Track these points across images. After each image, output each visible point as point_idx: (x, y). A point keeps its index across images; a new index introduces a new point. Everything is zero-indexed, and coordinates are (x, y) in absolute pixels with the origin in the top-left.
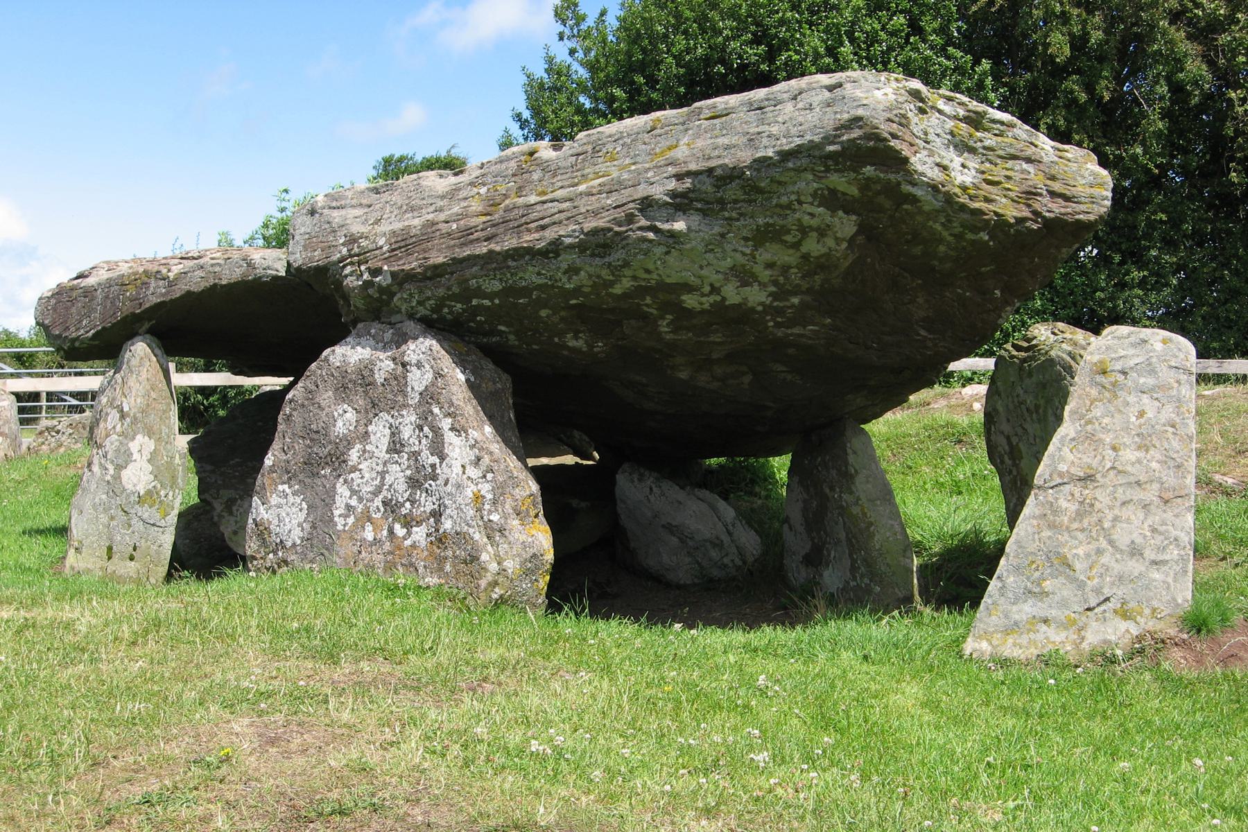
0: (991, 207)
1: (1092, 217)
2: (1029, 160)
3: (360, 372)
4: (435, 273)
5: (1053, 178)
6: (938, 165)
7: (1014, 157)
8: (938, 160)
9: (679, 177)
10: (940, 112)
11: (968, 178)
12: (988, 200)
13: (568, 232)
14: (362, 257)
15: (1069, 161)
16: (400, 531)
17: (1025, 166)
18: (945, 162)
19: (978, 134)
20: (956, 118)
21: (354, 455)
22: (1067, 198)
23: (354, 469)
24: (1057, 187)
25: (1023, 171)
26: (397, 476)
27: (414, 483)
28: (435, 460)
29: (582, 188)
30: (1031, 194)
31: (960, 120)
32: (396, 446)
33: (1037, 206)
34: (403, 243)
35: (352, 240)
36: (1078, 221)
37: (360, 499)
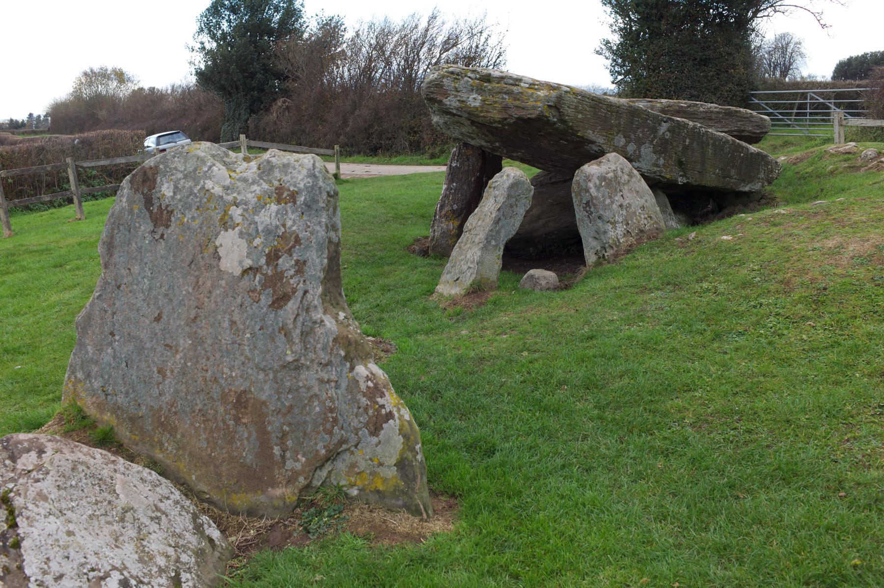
0: (489, 115)
1: (533, 116)
2: (506, 93)
5: (518, 100)
6: (459, 101)
7: (500, 93)
8: (459, 98)
10: (470, 77)
11: (477, 104)
12: (487, 112)
15: (536, 89)
17: (505, 96)
18: (464, 99)
19: (485, 84)
20: (476, 79)
22: (523, 108)
24: (517, 103)
25: (503, 98)
30: (506, 108)
31: (478, 79)
33: (509, 112)
36: (529, 118)
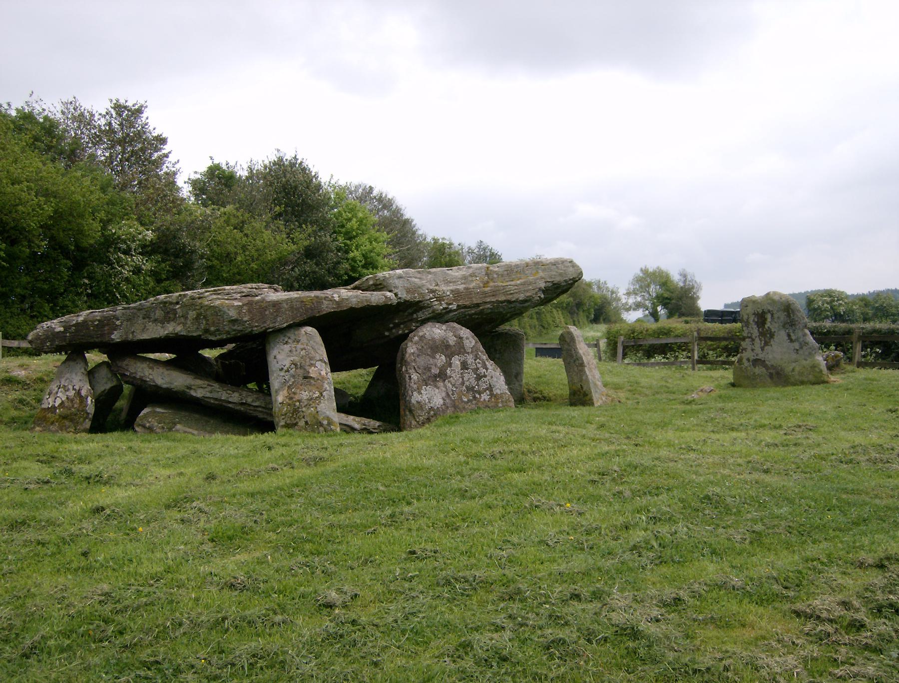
3: (443, 342)
4: (478, 305)
9: (546, 282)
13: (522, 297)
14: (440, 299)
16: (477, 396)
21: (448, 371)
23: (450, 377)
26: (470, 378)
27: (479, 378)
28: (484, 370)
29: (518, 282)
32: (464, 366)
34: (457, 294)
35: (432, 291)
37: (456, 388)
